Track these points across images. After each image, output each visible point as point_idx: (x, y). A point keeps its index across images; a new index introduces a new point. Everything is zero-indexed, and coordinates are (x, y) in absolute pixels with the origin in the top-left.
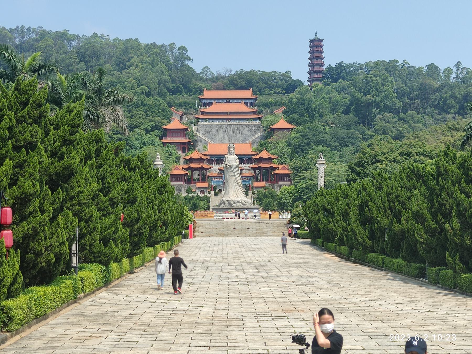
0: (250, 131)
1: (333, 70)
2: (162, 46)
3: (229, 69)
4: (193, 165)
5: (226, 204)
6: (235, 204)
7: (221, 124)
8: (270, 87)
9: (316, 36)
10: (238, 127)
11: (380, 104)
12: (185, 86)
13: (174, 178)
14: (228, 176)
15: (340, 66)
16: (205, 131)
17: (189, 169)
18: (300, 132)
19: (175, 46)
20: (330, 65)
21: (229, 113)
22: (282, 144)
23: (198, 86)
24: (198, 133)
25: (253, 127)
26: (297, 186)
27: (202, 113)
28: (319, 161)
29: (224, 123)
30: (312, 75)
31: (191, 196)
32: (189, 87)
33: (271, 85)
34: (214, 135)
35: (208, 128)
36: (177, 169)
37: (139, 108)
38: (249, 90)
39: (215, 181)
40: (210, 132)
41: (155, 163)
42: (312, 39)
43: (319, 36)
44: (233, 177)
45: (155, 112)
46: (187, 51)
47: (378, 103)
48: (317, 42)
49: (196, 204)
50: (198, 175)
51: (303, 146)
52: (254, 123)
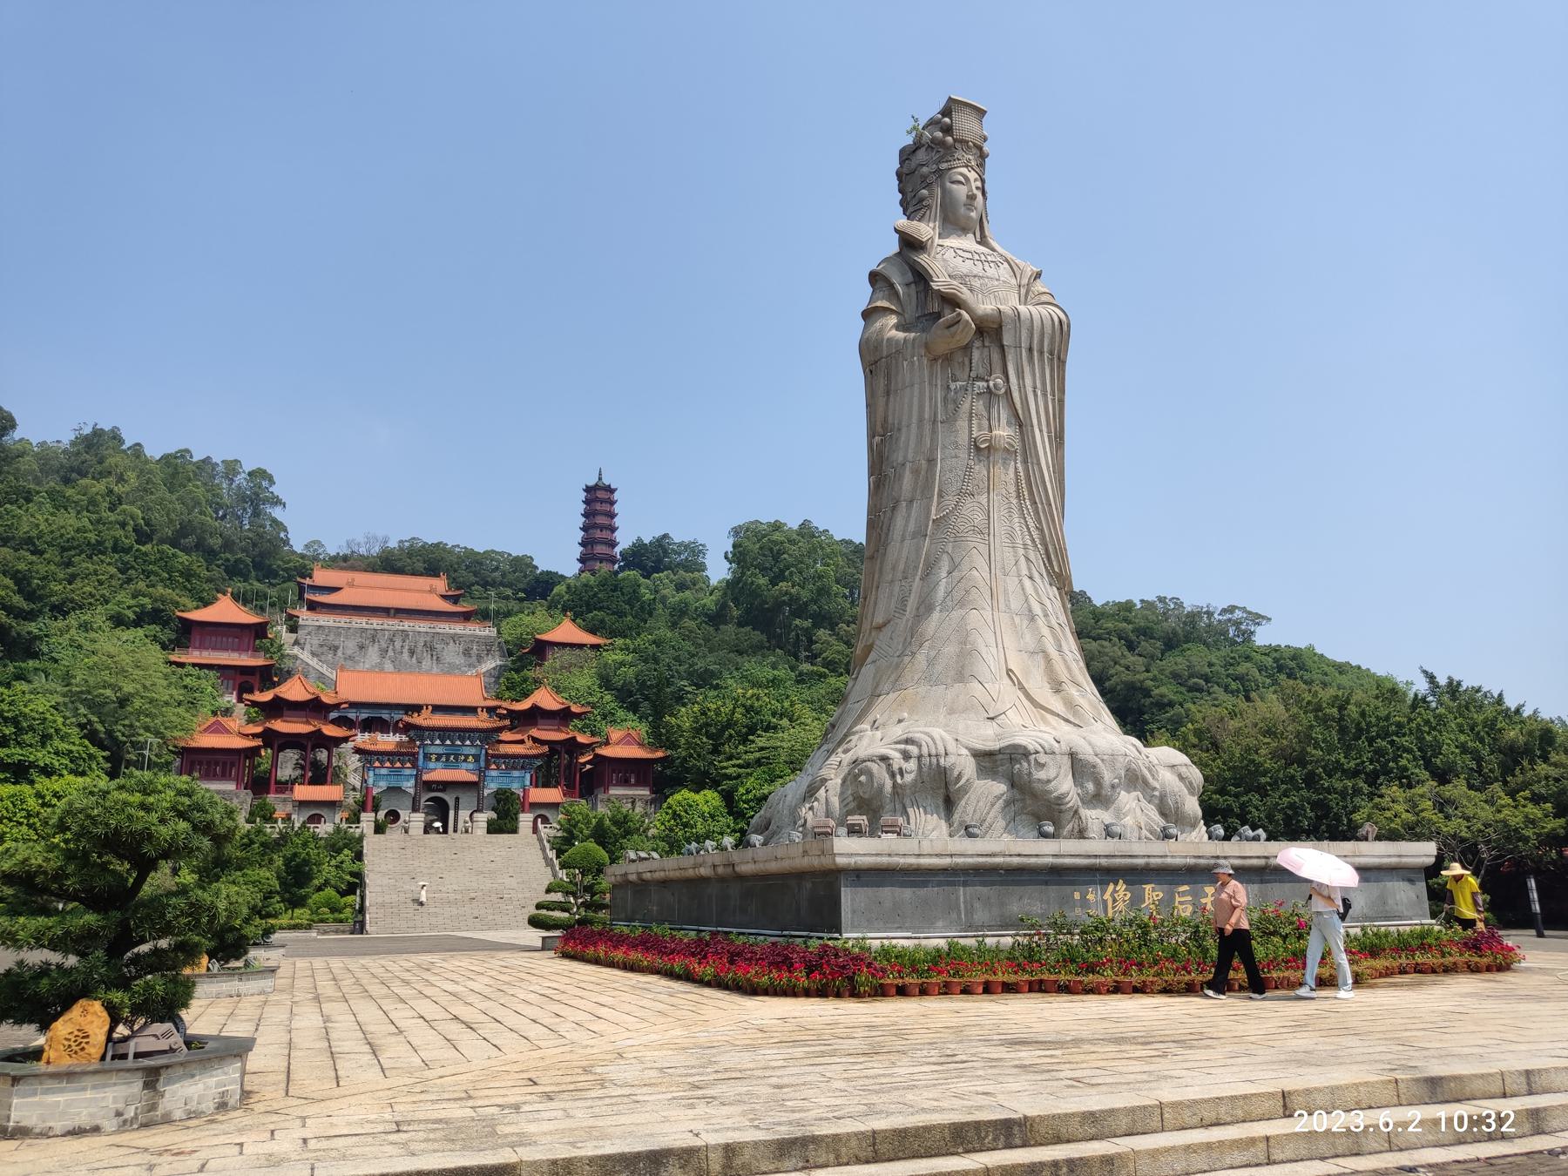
0: (464, 654)
1: (647, 549)
2: (207, 461)
3: (380, 534)
4: (280, 726)
5: (967, 809)
6: (1099, 798)
7: (375, 626)
8: (486, 585)
9: (600, 479)
10: (428, 639)
11: (809, 608)
12: (257, 566)
13: (200, 763)
14: (952, 460)
15: (662, 543)
16: (321, 646)
18: (634, 651)
19: (241, 467)
20: (639, 539)
21: (392, 612)
22: (584, 680)
24: (296, 650)
25: (472, 641)
26: (742, 790)
29: (385, 627)
30: (588, 564)
31: (273, 831)
32: (270, 566)
33: (489, 579)
34: (351, 658)
36: (218, 729)
37: (103, 557)
38: (439, 576)
39: (384, 771)
40: (336, 649)
42: (592, 483)
43: (606, 481)
44: (1006, 475)
45: (157, 574)
46: (272, 482)
47: (806, 604)
48: (603, 492)
49: (306, 862)
50: (298, 766)
52: (478, 632)
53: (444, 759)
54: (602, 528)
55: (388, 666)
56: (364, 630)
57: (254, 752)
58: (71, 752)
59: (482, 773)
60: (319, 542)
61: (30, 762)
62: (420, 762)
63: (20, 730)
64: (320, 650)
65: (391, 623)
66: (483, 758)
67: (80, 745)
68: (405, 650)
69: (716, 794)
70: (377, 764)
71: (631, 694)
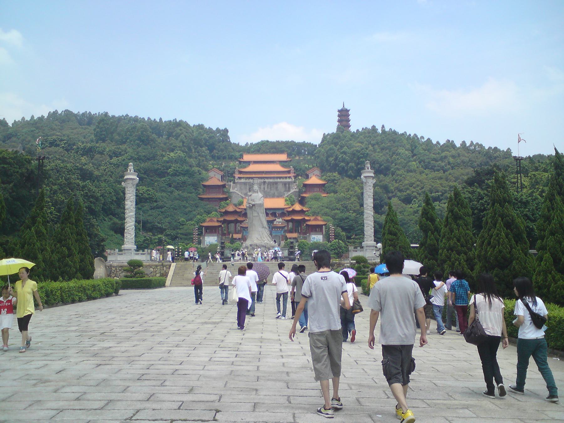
9: (344, 106)
17: (224, 222)
27: (241, 172)
28: (364, 172)
36: (211, 221)
41: (126, 177)
42: (340, 109)
43: (346, 107)
57: (220, 226)
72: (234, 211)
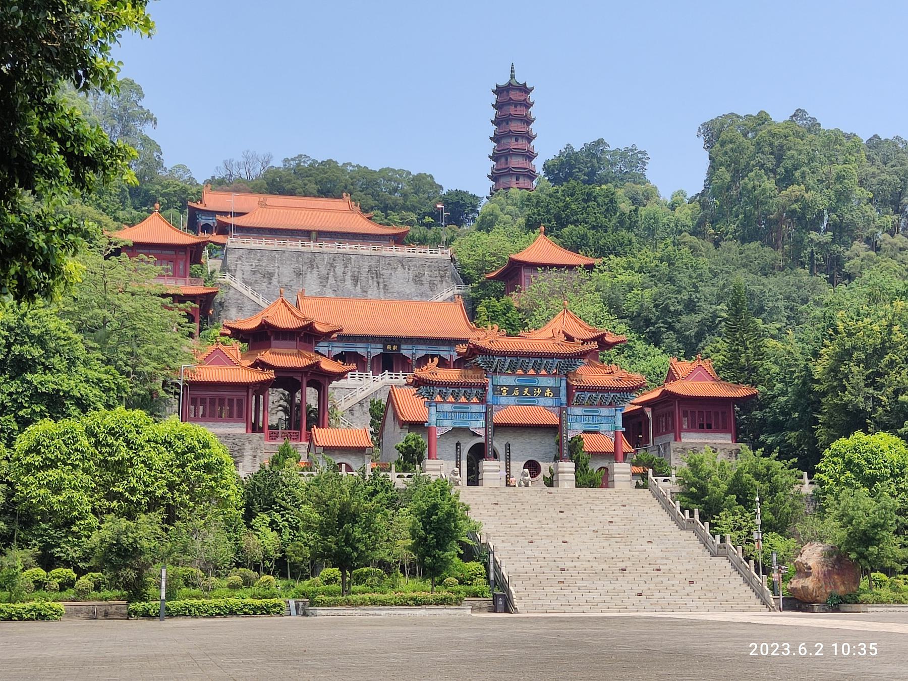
0: (415, 282)
7: (312, 249)
9: (512, 77)
10: (373, 263)
13: (203, 402)
21: (314, 235)
23: (177, 188)
35: (264, 262)
39: (447, 408)
40: (269, 276)
42: (504, 81)
43: (520, 79)
48: (518, 92)
51: (678, 313)
52: (428, 254)
53: (516, 393)
54: (518, 136)
55: (329, 294)
56: (300, 253)
58: (100, 380)
59: (562, 411)
60: (184, 167)
61: (65, 392)
62: (490, 396)
63: (48, 354)
64: (253, 278)
65: (330, 245)
66: (563, 392)
67: (107, 372)
68: (348, 277)
69: (895, 439)
70: (438, 398)
71: (648, 322)
72: (304, 328)
